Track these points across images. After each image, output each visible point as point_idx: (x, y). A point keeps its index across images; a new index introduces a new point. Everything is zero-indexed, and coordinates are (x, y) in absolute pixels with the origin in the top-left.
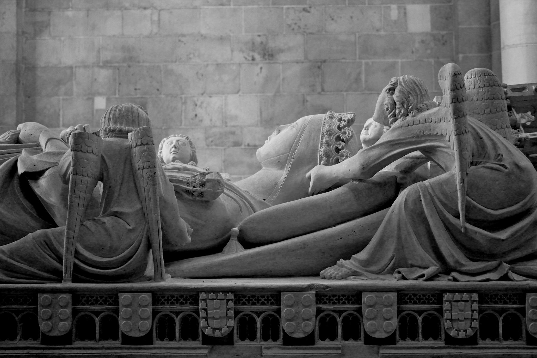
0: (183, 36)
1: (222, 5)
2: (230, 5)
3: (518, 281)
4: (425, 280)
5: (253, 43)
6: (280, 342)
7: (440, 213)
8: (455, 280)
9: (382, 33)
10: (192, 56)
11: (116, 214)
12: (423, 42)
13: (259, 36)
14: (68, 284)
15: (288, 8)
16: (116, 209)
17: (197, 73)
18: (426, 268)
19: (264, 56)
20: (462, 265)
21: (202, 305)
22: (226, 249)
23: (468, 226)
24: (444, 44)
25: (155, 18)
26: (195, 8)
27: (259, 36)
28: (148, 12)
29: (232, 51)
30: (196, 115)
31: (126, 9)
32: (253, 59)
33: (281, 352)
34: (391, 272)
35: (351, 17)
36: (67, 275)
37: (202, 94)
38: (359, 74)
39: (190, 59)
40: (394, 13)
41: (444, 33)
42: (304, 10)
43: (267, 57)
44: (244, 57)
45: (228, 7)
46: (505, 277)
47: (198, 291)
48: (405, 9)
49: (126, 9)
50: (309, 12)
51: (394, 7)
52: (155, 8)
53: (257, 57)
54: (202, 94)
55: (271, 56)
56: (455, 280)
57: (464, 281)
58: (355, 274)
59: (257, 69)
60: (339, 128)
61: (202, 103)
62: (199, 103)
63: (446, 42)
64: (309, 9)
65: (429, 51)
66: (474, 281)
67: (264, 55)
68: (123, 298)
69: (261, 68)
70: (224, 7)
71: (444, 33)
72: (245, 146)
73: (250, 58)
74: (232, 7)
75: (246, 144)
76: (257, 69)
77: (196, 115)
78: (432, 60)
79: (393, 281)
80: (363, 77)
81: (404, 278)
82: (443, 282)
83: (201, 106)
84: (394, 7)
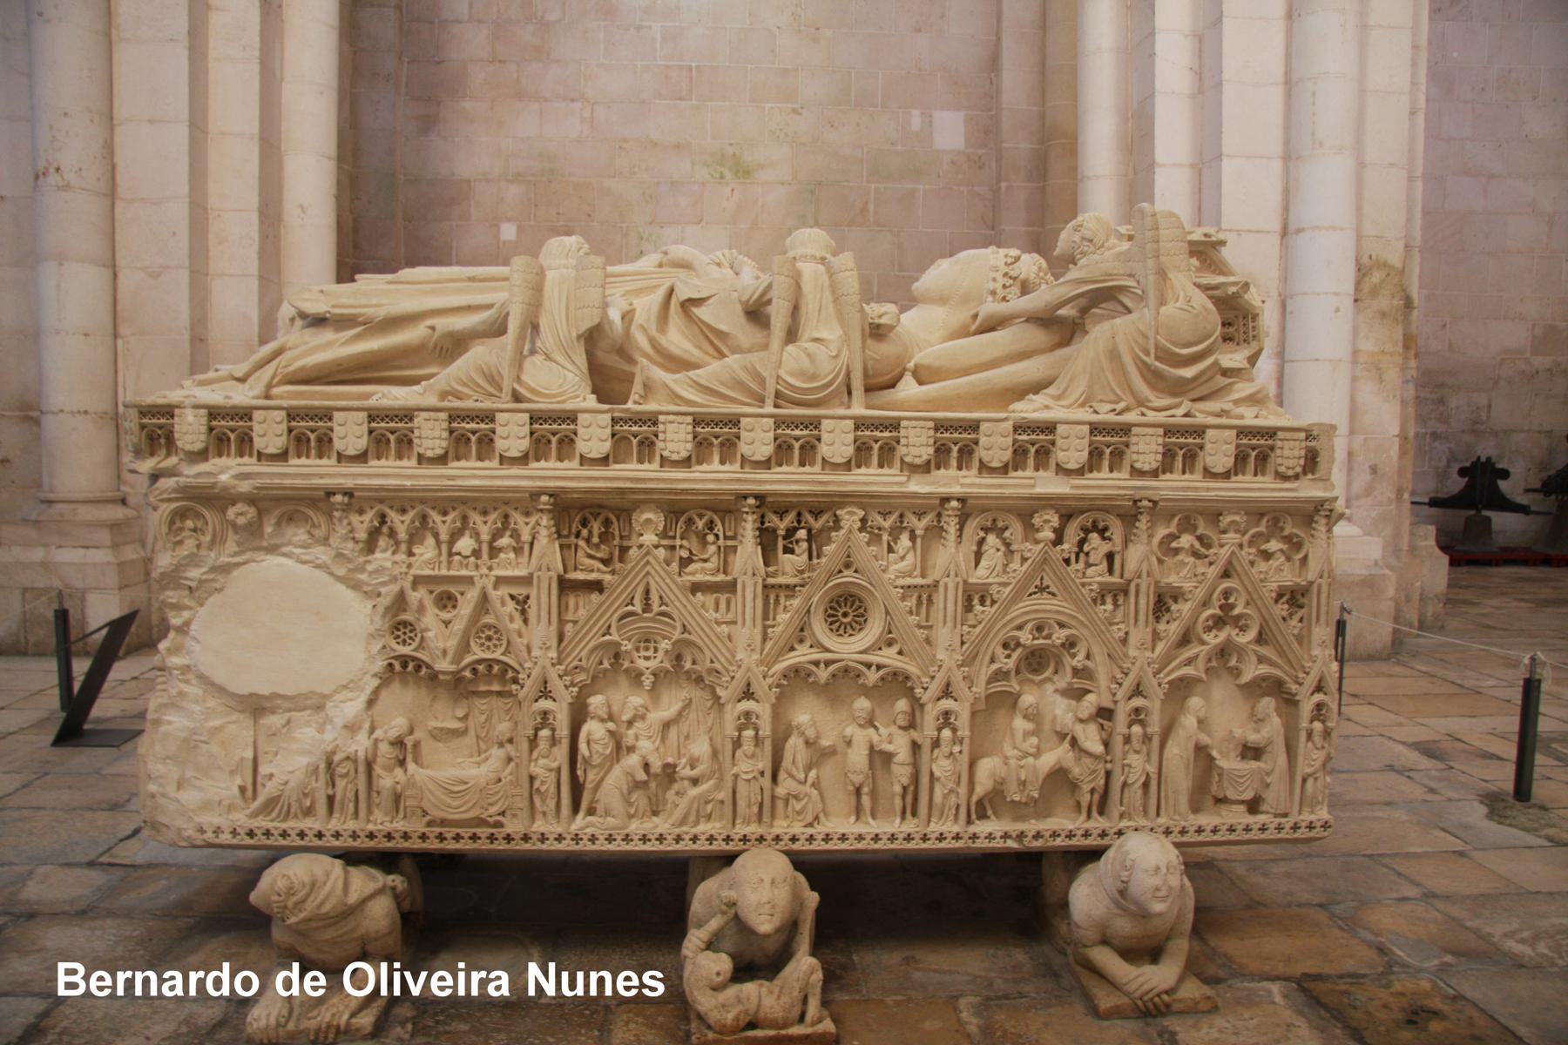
0: (626, 141)
1: (680, 99)
3: (1200, 419)
4: (1118, 414)
5: (723, 155)
6: (974, 471)
7: (1132, 350)
8: (1143, 415)
9: (899, 148)
10: (636, 169)
11: (816, 340)
12: (953, 162)
14: (769, 409)
16: (816, 335)
18: (1117, 403)
19: (736, 173)
20: (1149, 401)
21: (903, 432)
22: (901, 385)
23: (1157, 364)
24: (980, 168)
25: (587, 114)
26: (643, 102)
28: (577, 105)
29: (693, 164)
31: (546, 100)
32: (722, 177)
33: (978, 481)
34: (1082, 405)
35: (858, 124)
36: (770, 401)
37: (651, 223)
38: (866, 203)
40: (916, 121)
41: (981, 152)
42: (794, 111)
43: (741, 174)
46: (1186, 415)
49: (546, 100)
51: (916, 113)
52: (587, 100)
53: (728, 175)
54: (651, 223)
55: (747, 173)
56: (1143, 415)
57: (1152, 416)
58: (1047, 407)
59: (727, 190)
60: (1006, 264)
61: (650, 235)
62: (645, 236)
65: (960, 176)
66: (1161, 417)
67: (738, 171)
68: (826, 424)
71: (981, 152)
76: (727, 190)
78: (965, 189)
79: (1085, 415)
80: (871, 207)
81: (1096, 412)
82: (1131, 417)
83: (647, 240)
84: (916, 113)
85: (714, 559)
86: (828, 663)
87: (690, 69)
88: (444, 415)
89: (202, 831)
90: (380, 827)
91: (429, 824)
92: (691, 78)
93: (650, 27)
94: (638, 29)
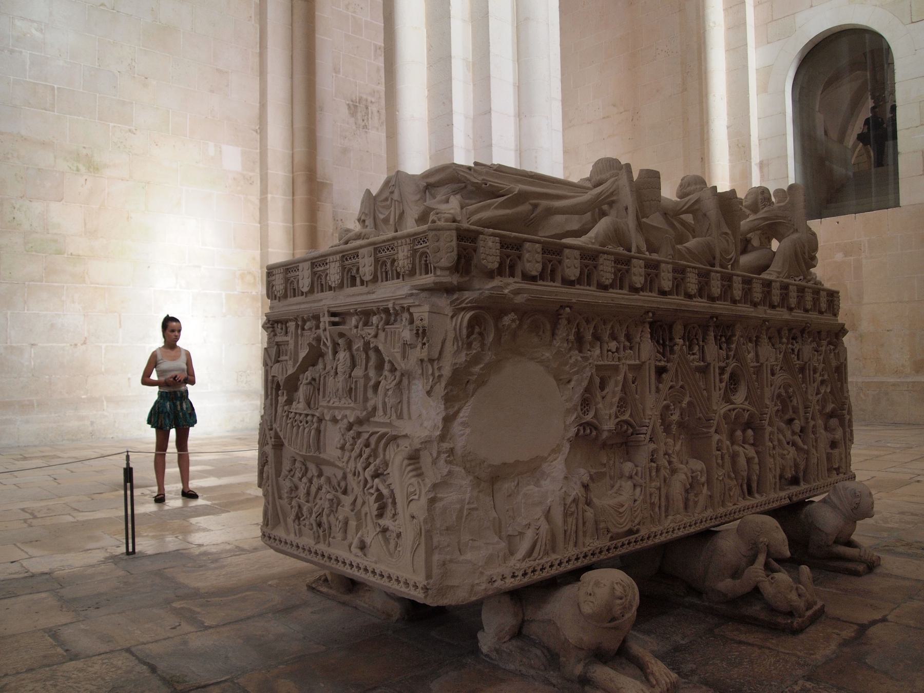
2: (54, 111)
10: (9, 156)
13: (84, 148)
15: (114, 126)
17: (16, 175)
27: (84, 148)
29: (55, 157)
30: (14, 218)
32: (78, 170)
35: (174, 146)
37: (21, 197)
39: (8, 158)
41: (251, 174)
42: (130, 130)
44: (68, 166)
45: (52, 113)
47: (753, 278)
48: (220, 148)
50: (134, 134)
53: (83, 169)
54: (21, 197)
55: (97, 169)
62: (17, 206)
63: (253, 182)
64: (134, 131)
69: (86, 180)
70: (48, 112)
72: (68, 255)
73: (75, 168)
74: (56, 113)
75: (69, 253)
77: (14, 218)
83: (19, 209)
85: (697, 353)
86: (734, 410)
87: (53, 88)
88: (612, 258)
89: (491, 581)
90: (589, 548)
91: (612, 539)
92: (54, 95)
93: (21, 52)
94: (12, 52)
